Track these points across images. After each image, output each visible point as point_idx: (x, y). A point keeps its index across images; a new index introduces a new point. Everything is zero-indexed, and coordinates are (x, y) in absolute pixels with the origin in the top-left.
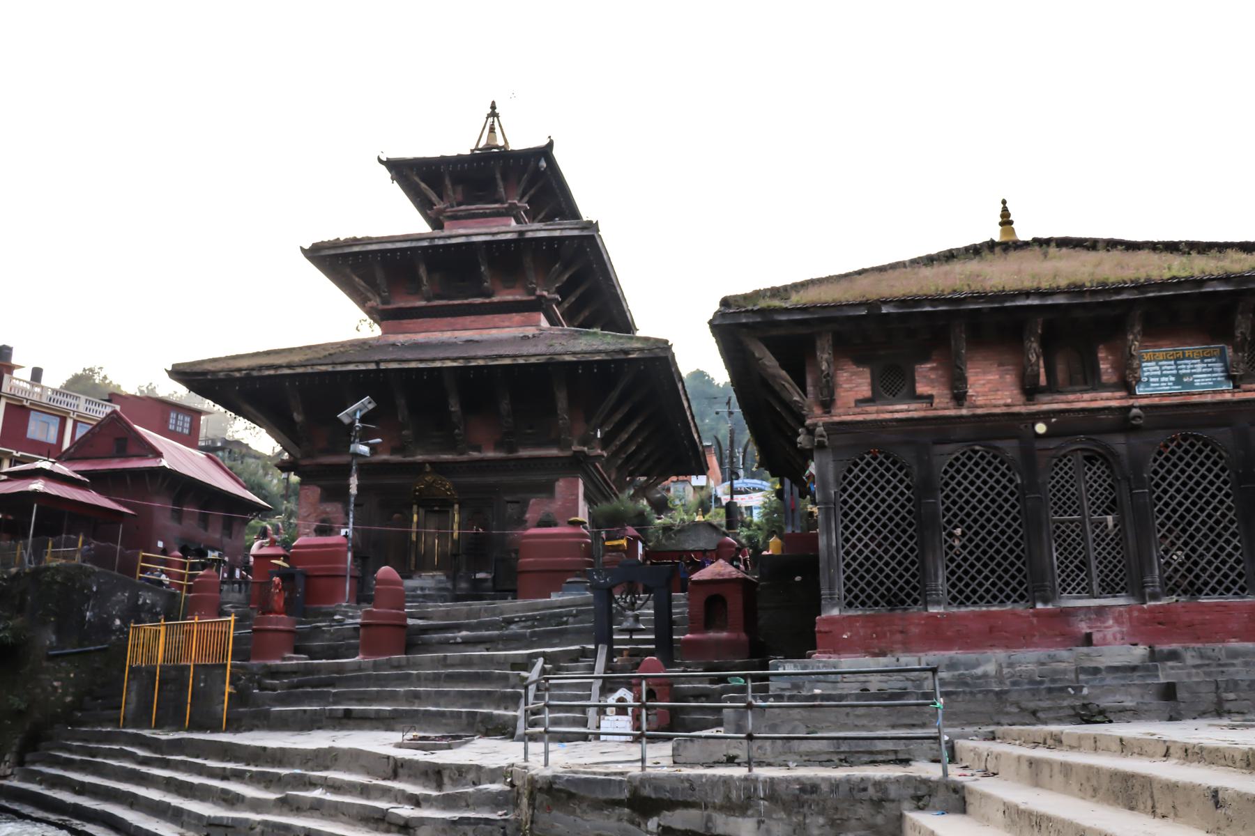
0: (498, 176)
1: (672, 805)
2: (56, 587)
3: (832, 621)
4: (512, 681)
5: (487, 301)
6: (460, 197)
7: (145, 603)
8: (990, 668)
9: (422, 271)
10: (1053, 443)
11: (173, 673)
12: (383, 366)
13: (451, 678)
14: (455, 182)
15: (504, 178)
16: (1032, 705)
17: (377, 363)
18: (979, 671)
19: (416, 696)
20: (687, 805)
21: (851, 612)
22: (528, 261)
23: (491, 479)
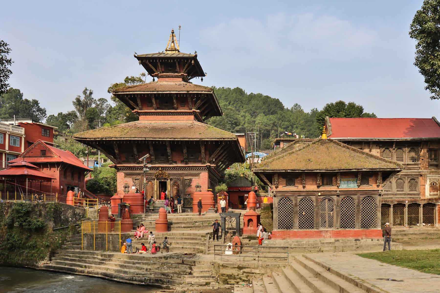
0: (177, 64)
1: (245, 268)
2: (53, 209)
3: (275, 232)
4: (203, 240)
5: (176, 111)
6: (163, 70)
7: (77, 213)
8: (304, 242)
9: (154, 101)
10: (322, 197)
11: (100, 236)
12: (147, 139)
13: (185, 239)
14: (161, 64)
15: (179, 64)
16: (310, 250)
17: (145, 138)
18: (302, 243)
19: (178, 243)
20: (247, 268)
21: (279, 230)
22: (189, 100)
23: (180, 172)
